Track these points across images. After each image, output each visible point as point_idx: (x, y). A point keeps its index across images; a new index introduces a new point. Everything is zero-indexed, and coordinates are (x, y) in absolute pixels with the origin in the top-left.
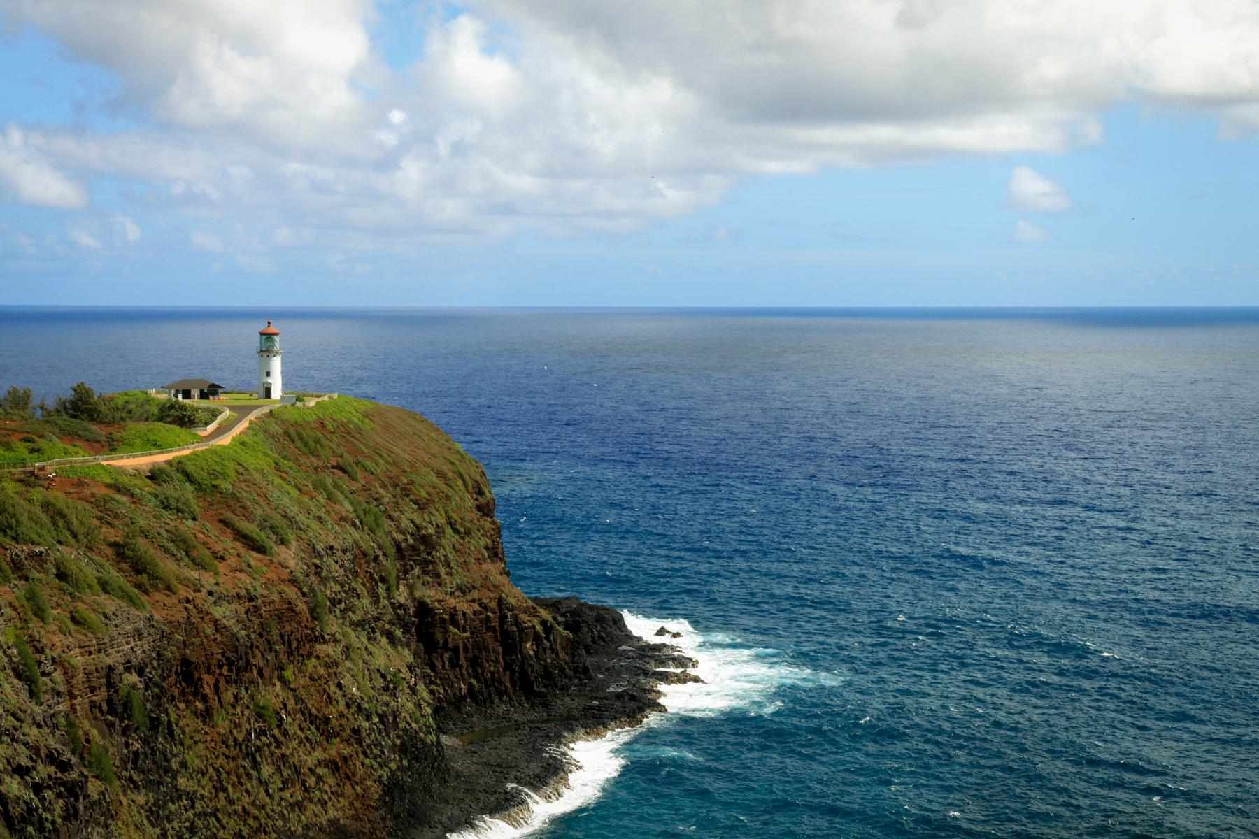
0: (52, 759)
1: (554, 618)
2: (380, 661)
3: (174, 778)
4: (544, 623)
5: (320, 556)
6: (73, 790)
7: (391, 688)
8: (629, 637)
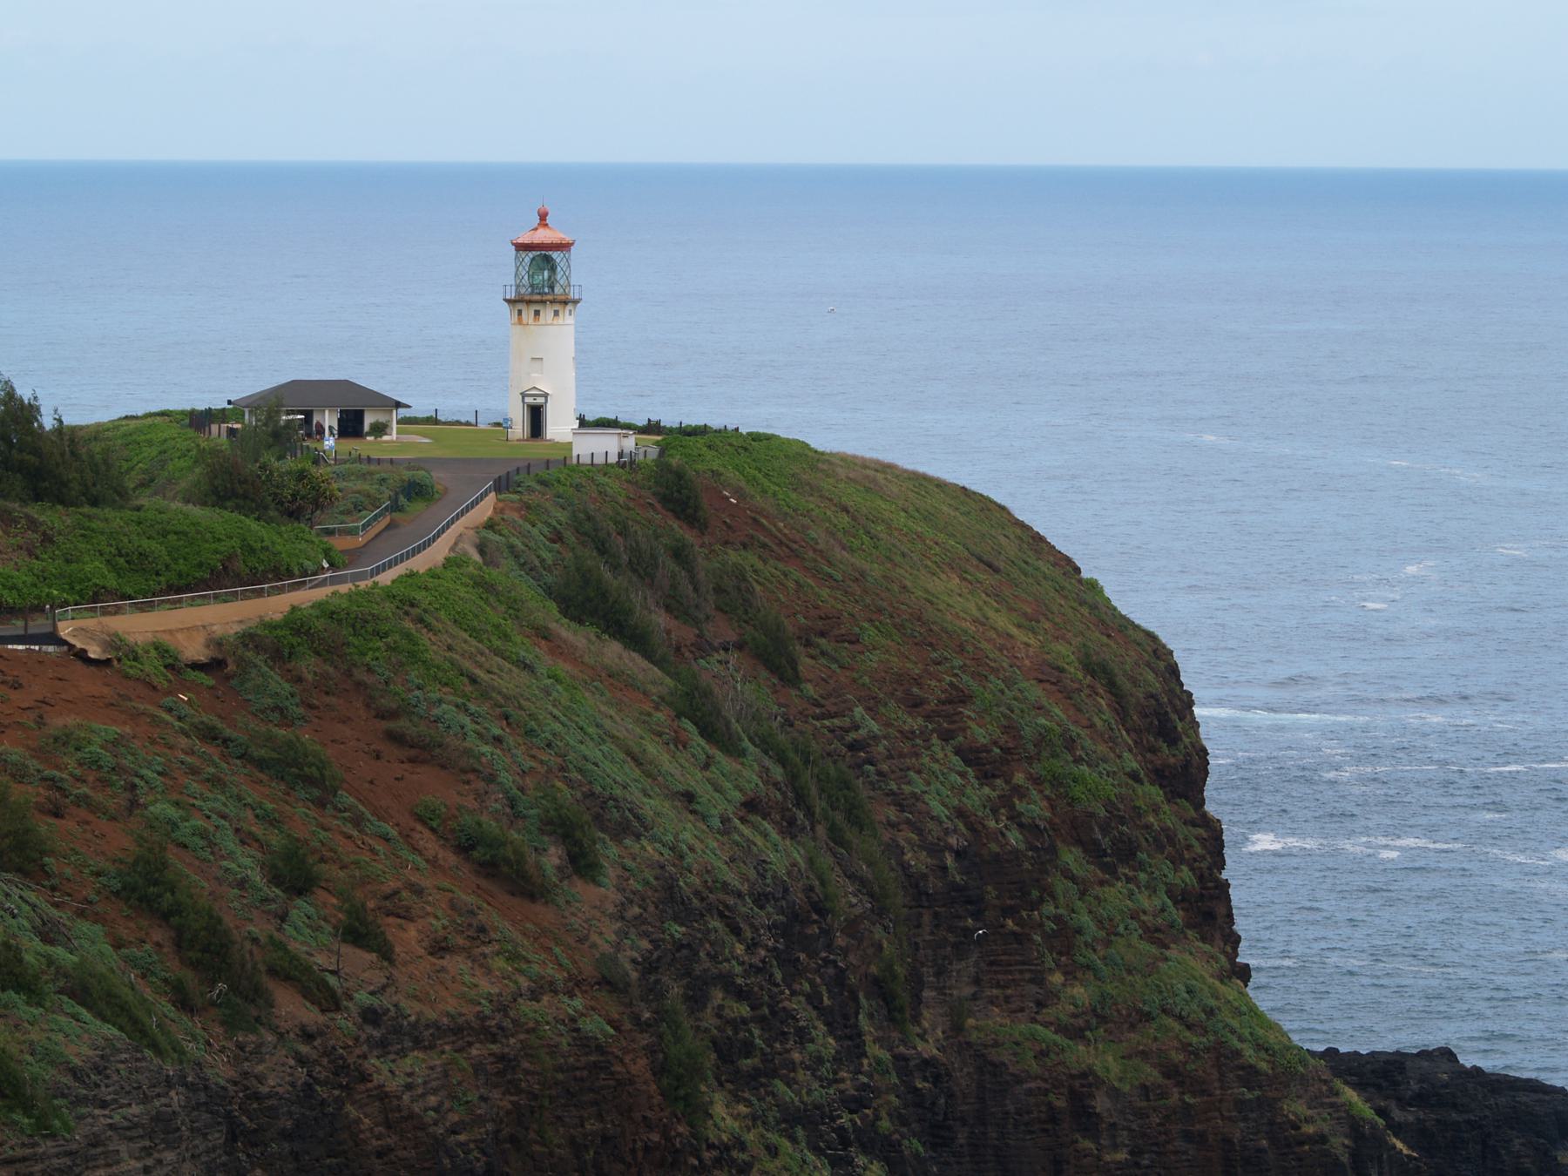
1: (1381, 1112)
4: (1355, 1126)
5: (684, 913)
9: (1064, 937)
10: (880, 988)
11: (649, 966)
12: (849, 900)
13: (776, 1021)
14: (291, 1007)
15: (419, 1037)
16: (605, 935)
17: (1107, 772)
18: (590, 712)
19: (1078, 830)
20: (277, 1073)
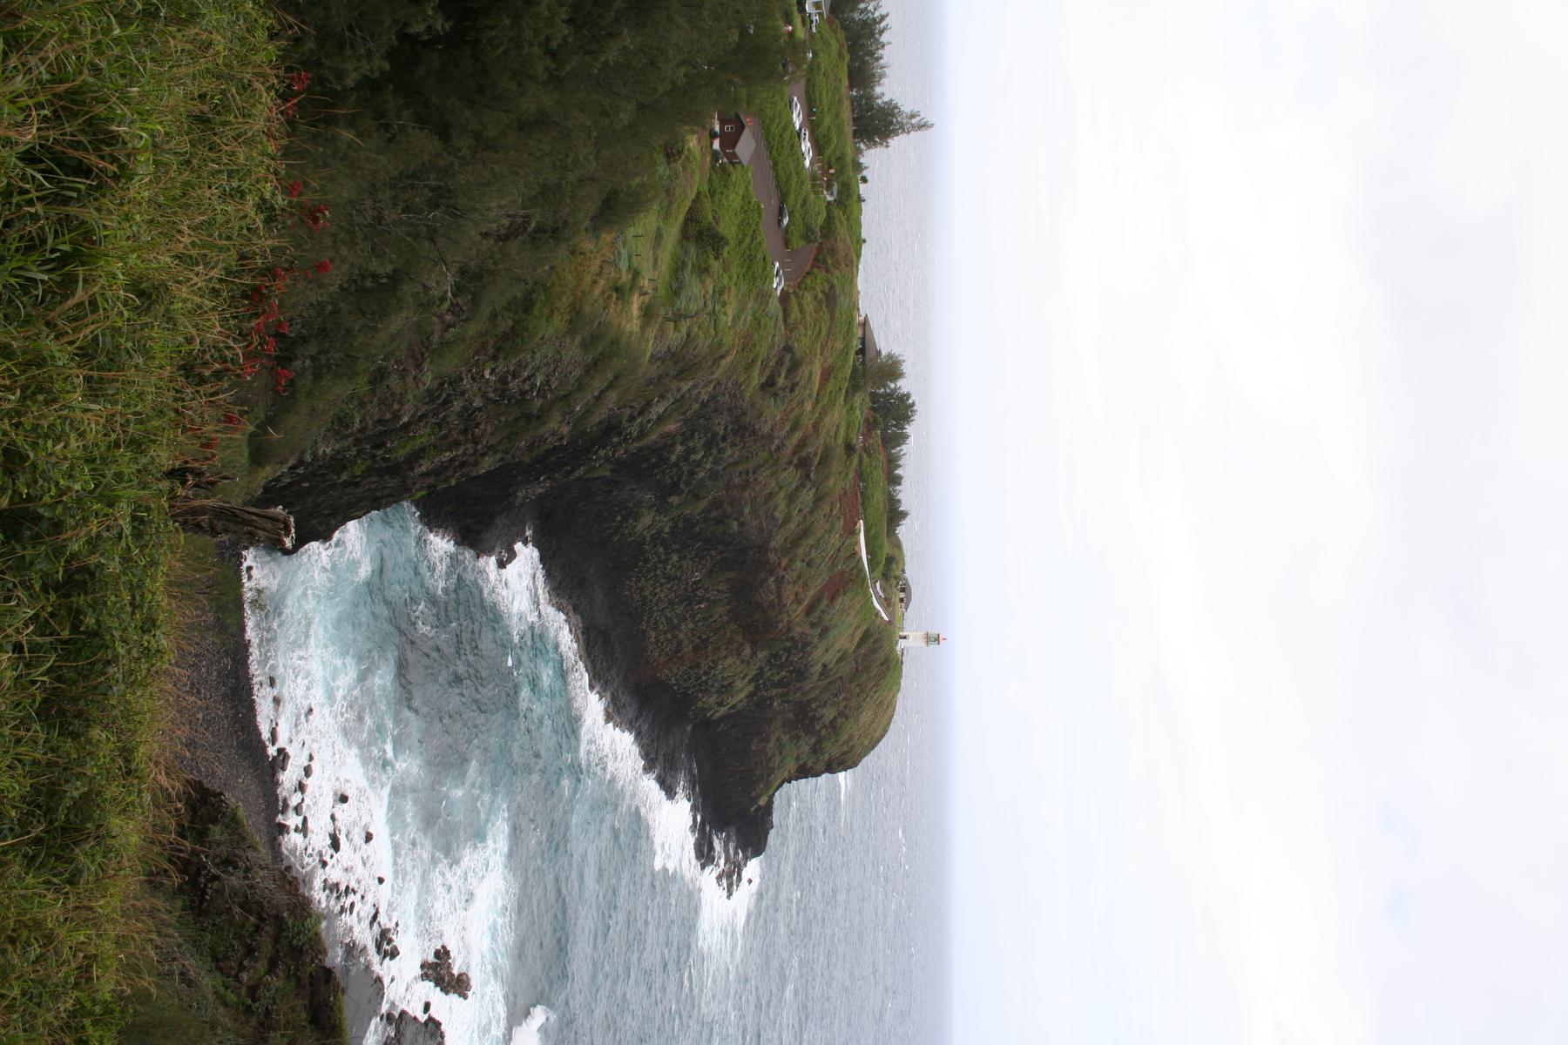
0: (692, 473)
2: (739, 684)
3: (677, 551)
6: (674, 488)
7: (726, 689)
8: (746, 859)
9: (798, 737)
10: (787, 694)
11: (792, 639)
12: (807, 686)
13: (781, 667)
14: (784, 562)
15: (778, 588)
16: (799, 629)
17: (832, 750)
18: (844, 638)
19: (820, 741)
20: (772, 557)
